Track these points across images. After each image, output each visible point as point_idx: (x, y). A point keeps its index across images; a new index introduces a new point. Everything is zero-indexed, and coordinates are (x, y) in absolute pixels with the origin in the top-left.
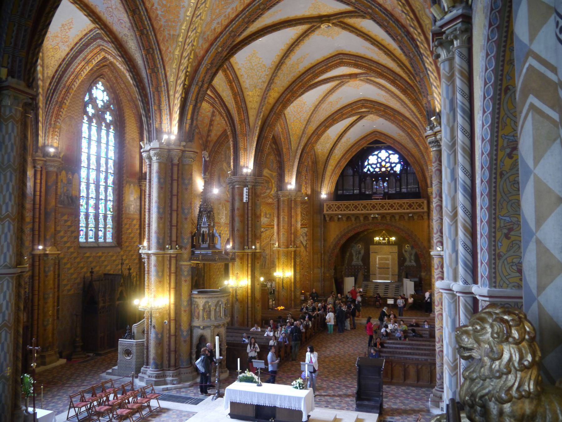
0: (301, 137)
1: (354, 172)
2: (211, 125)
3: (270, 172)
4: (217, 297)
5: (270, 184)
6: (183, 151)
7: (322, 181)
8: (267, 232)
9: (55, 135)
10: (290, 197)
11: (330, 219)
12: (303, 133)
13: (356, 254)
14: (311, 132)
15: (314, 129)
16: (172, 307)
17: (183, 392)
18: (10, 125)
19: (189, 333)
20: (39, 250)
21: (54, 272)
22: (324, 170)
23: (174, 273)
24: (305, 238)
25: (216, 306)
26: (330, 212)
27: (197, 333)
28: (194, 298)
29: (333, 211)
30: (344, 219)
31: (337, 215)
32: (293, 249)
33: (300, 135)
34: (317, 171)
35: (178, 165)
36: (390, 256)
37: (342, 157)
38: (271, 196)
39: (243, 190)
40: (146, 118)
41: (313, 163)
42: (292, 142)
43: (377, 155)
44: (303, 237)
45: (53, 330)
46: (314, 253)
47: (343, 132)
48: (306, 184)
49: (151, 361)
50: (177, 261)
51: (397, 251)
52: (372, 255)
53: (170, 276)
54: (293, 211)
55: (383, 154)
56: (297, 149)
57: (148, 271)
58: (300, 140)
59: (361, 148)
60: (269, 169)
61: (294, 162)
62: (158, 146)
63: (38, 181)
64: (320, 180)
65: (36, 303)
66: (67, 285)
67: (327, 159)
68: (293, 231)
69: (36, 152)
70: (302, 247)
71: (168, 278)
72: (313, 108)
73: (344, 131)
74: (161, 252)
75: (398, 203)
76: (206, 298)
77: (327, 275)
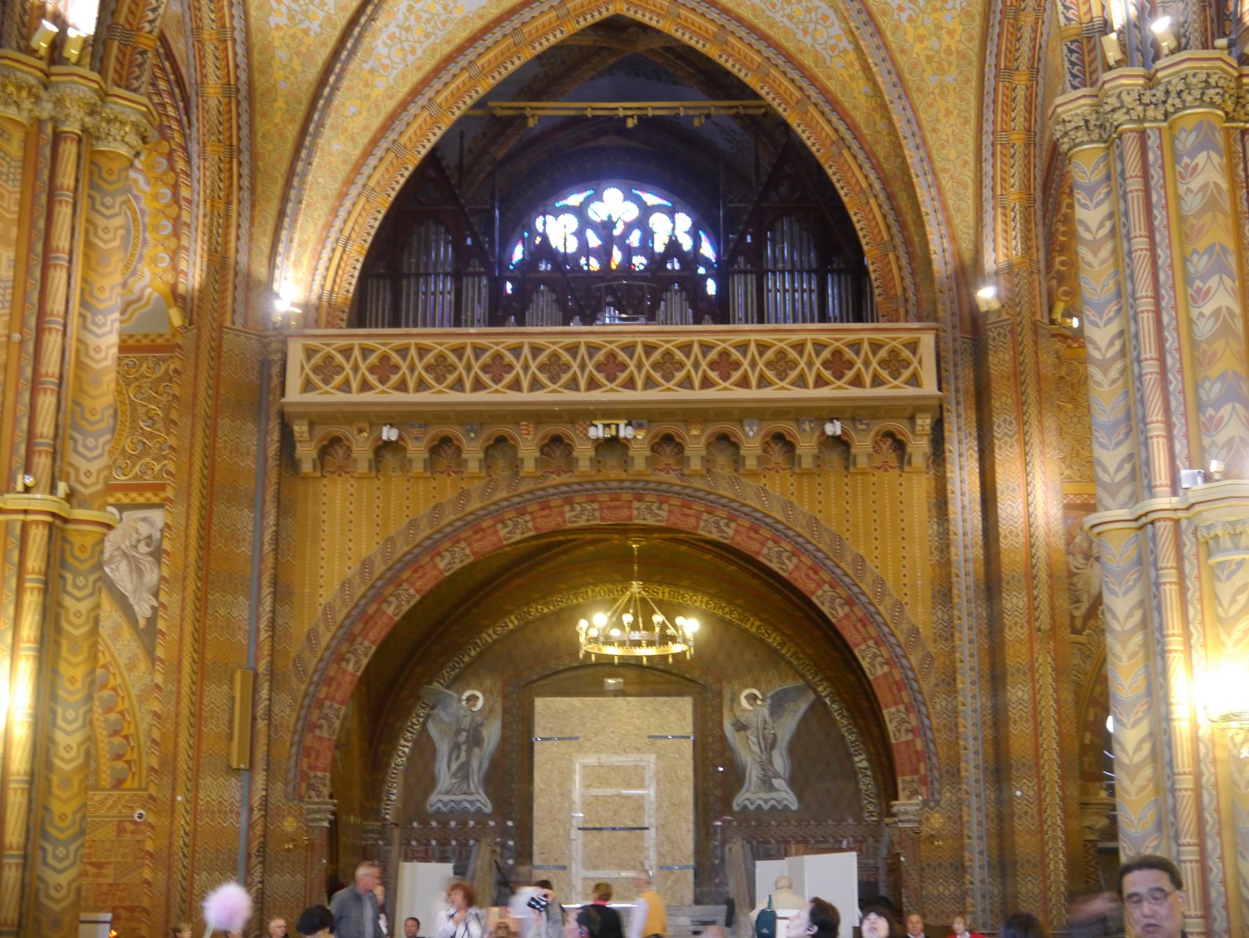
1: (462, 254)
7: (281, 214)
10: (46, 110)
11: (324, 452)
13: (457, 747)
22: (299, 146)
24: (151, 577)
26: (329, 395)
29: (345, 387)
30: (417, 450)
32: (40, 500)
34: (254, 157)
36: (651, 758)
37: (415, 92)
41: (230, 90)
44: (137, 570)
46: (202, 672)
48: (176, 234)
51: (689, 729)
52: (542, 753)
54: (64, 212)
59: (528, 54)
64: (272, 209)
67: (322, 82)
68: (51, 366)
70: (127, 633)
75: (763, 348)
77: (290, 824)
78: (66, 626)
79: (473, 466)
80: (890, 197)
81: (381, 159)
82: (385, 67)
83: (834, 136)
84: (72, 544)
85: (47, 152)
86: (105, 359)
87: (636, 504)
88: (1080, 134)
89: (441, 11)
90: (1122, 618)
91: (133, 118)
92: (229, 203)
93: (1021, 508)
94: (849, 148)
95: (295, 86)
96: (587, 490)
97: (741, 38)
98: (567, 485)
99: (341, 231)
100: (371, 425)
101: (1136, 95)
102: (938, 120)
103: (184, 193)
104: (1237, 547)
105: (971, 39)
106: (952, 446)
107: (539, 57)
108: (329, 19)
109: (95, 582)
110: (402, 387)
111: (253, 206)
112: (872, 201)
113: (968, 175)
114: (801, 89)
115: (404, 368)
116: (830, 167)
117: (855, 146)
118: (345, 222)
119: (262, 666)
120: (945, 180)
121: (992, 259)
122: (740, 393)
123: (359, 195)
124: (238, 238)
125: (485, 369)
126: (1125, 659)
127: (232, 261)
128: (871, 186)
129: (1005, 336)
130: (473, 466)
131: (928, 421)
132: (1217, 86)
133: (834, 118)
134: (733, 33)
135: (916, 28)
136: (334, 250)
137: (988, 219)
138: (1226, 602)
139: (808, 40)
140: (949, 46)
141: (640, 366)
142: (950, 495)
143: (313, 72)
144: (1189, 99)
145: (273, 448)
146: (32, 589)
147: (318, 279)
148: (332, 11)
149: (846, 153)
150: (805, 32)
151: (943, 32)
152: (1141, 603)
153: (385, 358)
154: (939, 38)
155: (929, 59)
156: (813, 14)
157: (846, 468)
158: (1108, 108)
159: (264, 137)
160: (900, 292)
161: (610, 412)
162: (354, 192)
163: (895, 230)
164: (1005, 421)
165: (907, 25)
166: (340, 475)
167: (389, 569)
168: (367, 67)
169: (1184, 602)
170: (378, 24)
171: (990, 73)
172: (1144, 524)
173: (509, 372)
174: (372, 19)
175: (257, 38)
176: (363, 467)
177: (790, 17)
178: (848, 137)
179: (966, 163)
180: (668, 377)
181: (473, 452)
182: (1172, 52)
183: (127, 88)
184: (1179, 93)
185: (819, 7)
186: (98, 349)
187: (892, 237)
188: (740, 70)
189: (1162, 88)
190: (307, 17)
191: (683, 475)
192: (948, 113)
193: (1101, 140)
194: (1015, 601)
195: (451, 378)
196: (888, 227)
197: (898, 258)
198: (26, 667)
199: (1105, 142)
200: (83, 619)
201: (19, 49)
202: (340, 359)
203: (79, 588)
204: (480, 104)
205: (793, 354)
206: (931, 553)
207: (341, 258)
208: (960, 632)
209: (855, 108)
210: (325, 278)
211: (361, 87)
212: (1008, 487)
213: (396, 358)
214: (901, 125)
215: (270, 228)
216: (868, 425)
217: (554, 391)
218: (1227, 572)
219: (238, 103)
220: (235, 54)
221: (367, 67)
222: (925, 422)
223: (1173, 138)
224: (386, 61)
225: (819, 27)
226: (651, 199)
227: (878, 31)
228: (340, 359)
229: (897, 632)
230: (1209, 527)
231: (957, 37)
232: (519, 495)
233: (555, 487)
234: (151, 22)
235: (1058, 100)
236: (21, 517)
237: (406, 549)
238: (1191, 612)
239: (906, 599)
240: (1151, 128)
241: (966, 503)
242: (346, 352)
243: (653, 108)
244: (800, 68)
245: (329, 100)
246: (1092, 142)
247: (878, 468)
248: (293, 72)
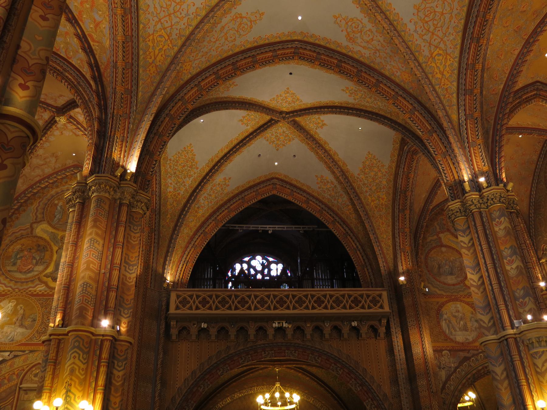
0: (168, 69)
3: (50, 229)
5: (48, 253)
7: (168, 252)
8: (17, 360)
12: (172, 63)
14: (187, 77)
15: (194, 72)
29: (191, 308)
30: (213, 331)
33: (164, 67)
37: (211, 215)
38: (45, 279)
42: (141, 83)
47: (222, 158)
54: (121, 229)
56: (150, 100)
58: (164, 76)
59: (246, 205)
60: (50, 225)
61: (141, 121)
67: (183, 210)
72: (204, 13)
73: (225, 155)
75: (331, 296)
78: (114, 382)
79: (232, 337)
80: (364, 251)
81: (199, 236)
82: (202, 206)
83: (345, 232)
84: (117, 349)
85: (117, 209)
86: (132, 282)
87: (287, 351)
88: (458, 214)
89: (221, 190)
90: (499, 374)
91: (145, 201)
92: (151, 247)
93: (420, 350)
94: (350, 235)
95: (174, 211)
96: (270, 346)
97: (314, 202)
98: (264, 344)
99: (186, 258)
100: (198, 322)
101: (477, 200)
102: (380, 226)
104: (540, 346)
105: (389, 201)
106: (393, 330)
107: (241, 212)
108: (186, 190)
109: (125, 364)
110: (210, 308)
111: (158, 249)
112: (358, 252)
113: (390, 242)
114: (333, 217)
115: (211, 302)
116: (344, 241)
117: (351, 235)
118: (187, 256)
120: (383, 244)
121: (400, 269)
122: (325, 311)
123: (192, 247)
124: (153, 259)
125: (239, 302)
126: (503, 390)
127: (151, 266)
128: (357, 247)
129: (409, 293)
130: (232, 337)
131: (386, 321)
132: (504, 197)
133: (344, 227)
134: (311, 200)
135: (371, 198)
136: (183, 265)
137: (399, 256)
138: (540, 366)
139: (336, 202)
140: (382, 203)
141: (291, 302)
142: (394, 346)
144: (496, 201)
145: (162, 331)
146: (104, 366)
147: (178, 274)
148: (188, 188)
149: (348, 237)
150: (335, 200)
151: (380, 199)
152: (505, 369)
153: (204, 299)
154: (379, 200)
155: (376, 207)
156: (338, 194)
157: (358, 338)
158: (468, 205)
159: (163, 226)
160: (369, 280)
161: (280, 318)
162: (190, 246)
163: (366, 261)
164: (411, 321)
165: (369, 197)
166: (184, 341)
167: (202, 374)
168: (197, 206)
169: (524, 368)
170: (202, 193)
171: (397, 211)
172: (504, 341)
173: (247, 304)
174: (201, 190)
175: (163, 195)
176: (194, 337)
177: (330, 195)
178: (349, 232)
179: (389, 239)
180: (301, 306)
181: (233, 332)
182: (487, 187)
183: (143, 191)
184: (492, 199)
185: (339, 192)
186: (130, 278)
187: (365, 263)
188: (313, 212)
189: (486, 198)
190: (179, 189)
191: (303, 341)
192: (383, 224)
193: (465, 216)
194: (422, 382)
195: (227, 306)
196: (364, 260)
197: (368, 270)
198: (99, 397)
199: (467, 216)
200: (120, 379)
201: (111, 175)
202: (189, 299)
203: (120, 367)
204: (224, 226)
205: (341, 298)
206: (388, 367)
207: (185, 267)
208: (403, 394)
209: (351, 223)
210: (180, 274)
211: (194, 212)
212: (415, 343)
213: (208, 299)
214: (368, 227)
215: (163, 256)
216: (366, 323)
217: (262, 310)
218: (538, 355)
219: (156, 215)
220: (156, 200)
221: (197, 206)
222: (384, 321)
223: (491, 214)
224: (202, 205)
225: (339, 198)
226: (271, 259)
227: (359, 199)
228: (189, 299)
229: (379, 396)
230: (529, 340)
231: (385, 200)
232: (247, 348)
233: (259, 345)
234: (152, 172)
235: (449, 204)
236: (101, 337)
237: (208, 367)
238: (527, 371)
239: (381, 384)
240: (483, 211)
241: (400, 349)
242: (191, 296)
243: (277, 227)
244: (333, 211)
245: (185, 215)
246: (462, 216)
247: (368, 338)
248: (174, 206)
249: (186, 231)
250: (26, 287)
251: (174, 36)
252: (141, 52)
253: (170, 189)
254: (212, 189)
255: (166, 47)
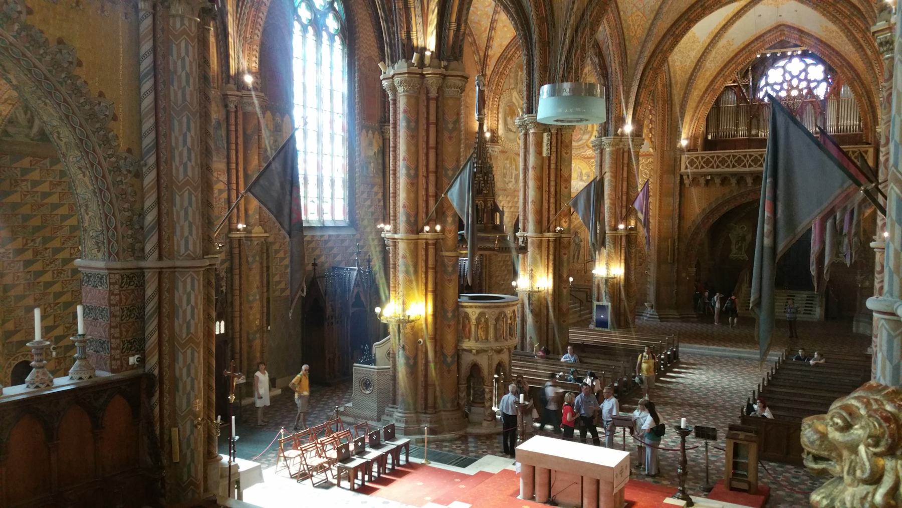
0: (645, 41)
2: (492, 28)
4: (498, 307)
6: (444, 77)
9: (253, 55)
10: (621, 146)
12: (648, 35)
16: (430, 319)
17: (446, 446)
18: (183, 45)
19: (456, 359)
20: (238, 230)
21: (261, 263)
23: (433, 268)
25: (497, 320)
27: (467, 359)
28: (463, 307)
30: (718, 181)
31: (705, 175)
35: (437, 99)
39: (542, 138)
40: (387, 23)
41: (664, 86)
43: (783, 67)
45: (262, 346)
47: (721, 29)
49: (399, 398)
50: (436, 250)
53: (426, 273)
55: (795, 66)
56: (637, 63)
57: (395, 264)
58: (643, 47)
62: (405, 70)
63: (233, 128)
65: (237, 308)
66: (279, 282)
67: (690, 79)
69: (228, 82)
71: (423, 276)
74: (414, 236)
76: (480, 307)
79: (734, 185)
103: (653, 112)
108: (692, 61)
110: (712, 167)
119: (676, 237)
143: (688, 76)
249: (695, 93)
250: (579, 152)
251: (647, 13)
252: (625, 30)
253: (678, 63)
254: (716, 53)
255: (643, 22)
